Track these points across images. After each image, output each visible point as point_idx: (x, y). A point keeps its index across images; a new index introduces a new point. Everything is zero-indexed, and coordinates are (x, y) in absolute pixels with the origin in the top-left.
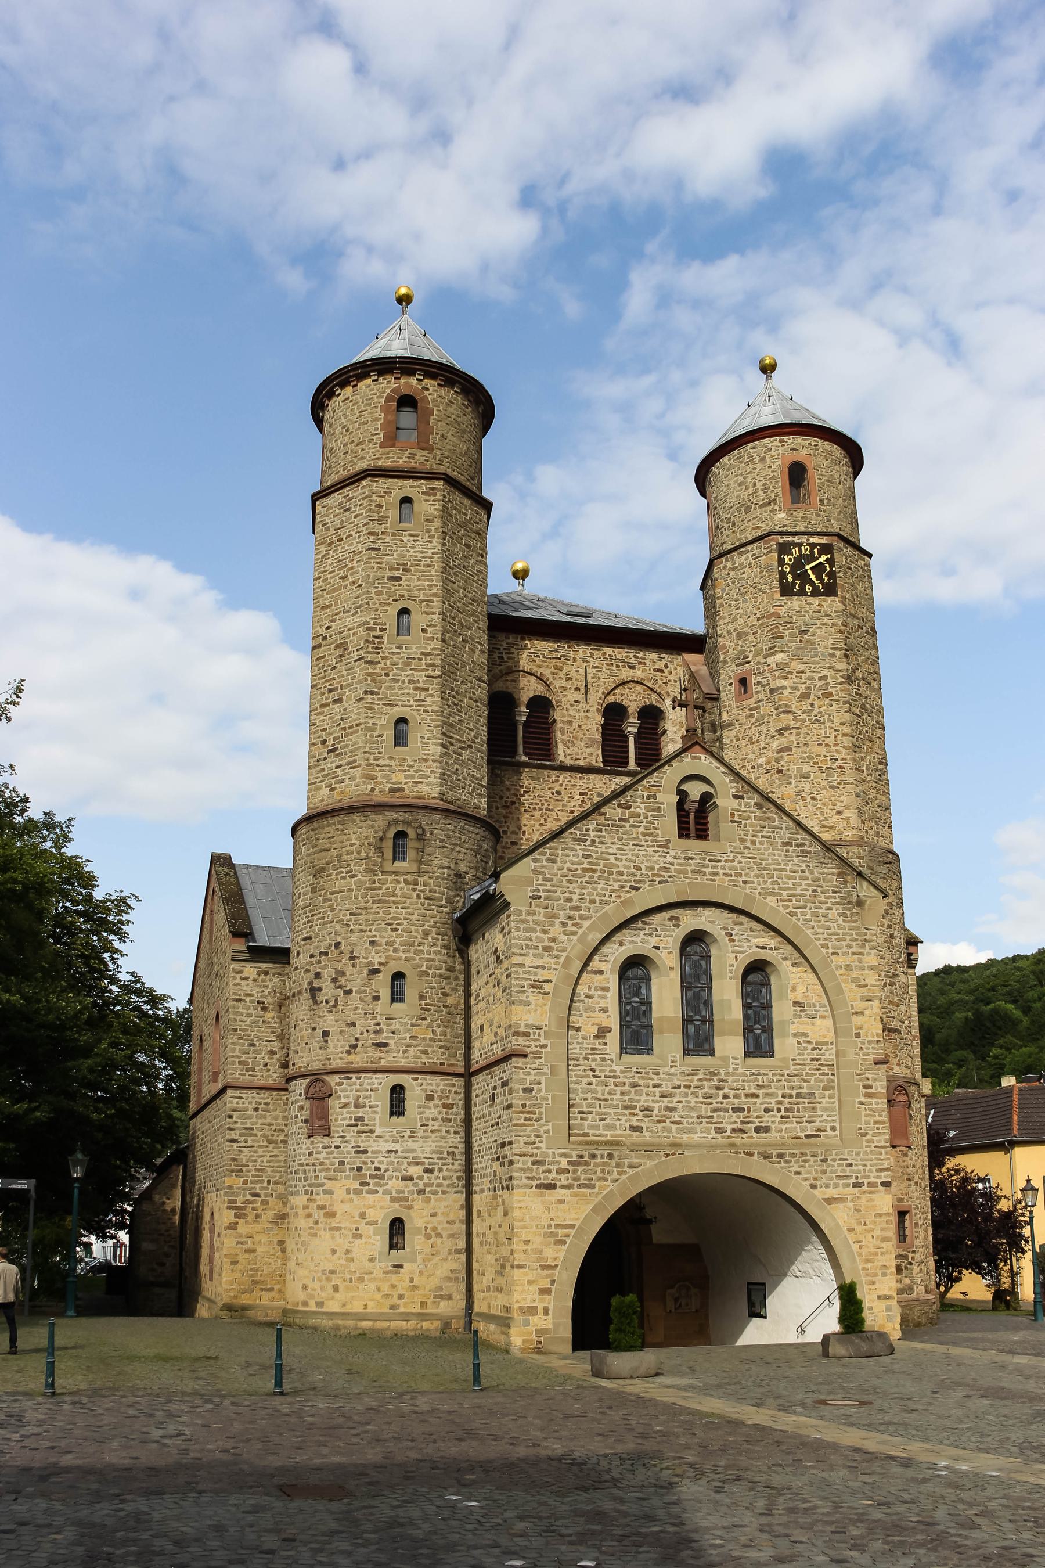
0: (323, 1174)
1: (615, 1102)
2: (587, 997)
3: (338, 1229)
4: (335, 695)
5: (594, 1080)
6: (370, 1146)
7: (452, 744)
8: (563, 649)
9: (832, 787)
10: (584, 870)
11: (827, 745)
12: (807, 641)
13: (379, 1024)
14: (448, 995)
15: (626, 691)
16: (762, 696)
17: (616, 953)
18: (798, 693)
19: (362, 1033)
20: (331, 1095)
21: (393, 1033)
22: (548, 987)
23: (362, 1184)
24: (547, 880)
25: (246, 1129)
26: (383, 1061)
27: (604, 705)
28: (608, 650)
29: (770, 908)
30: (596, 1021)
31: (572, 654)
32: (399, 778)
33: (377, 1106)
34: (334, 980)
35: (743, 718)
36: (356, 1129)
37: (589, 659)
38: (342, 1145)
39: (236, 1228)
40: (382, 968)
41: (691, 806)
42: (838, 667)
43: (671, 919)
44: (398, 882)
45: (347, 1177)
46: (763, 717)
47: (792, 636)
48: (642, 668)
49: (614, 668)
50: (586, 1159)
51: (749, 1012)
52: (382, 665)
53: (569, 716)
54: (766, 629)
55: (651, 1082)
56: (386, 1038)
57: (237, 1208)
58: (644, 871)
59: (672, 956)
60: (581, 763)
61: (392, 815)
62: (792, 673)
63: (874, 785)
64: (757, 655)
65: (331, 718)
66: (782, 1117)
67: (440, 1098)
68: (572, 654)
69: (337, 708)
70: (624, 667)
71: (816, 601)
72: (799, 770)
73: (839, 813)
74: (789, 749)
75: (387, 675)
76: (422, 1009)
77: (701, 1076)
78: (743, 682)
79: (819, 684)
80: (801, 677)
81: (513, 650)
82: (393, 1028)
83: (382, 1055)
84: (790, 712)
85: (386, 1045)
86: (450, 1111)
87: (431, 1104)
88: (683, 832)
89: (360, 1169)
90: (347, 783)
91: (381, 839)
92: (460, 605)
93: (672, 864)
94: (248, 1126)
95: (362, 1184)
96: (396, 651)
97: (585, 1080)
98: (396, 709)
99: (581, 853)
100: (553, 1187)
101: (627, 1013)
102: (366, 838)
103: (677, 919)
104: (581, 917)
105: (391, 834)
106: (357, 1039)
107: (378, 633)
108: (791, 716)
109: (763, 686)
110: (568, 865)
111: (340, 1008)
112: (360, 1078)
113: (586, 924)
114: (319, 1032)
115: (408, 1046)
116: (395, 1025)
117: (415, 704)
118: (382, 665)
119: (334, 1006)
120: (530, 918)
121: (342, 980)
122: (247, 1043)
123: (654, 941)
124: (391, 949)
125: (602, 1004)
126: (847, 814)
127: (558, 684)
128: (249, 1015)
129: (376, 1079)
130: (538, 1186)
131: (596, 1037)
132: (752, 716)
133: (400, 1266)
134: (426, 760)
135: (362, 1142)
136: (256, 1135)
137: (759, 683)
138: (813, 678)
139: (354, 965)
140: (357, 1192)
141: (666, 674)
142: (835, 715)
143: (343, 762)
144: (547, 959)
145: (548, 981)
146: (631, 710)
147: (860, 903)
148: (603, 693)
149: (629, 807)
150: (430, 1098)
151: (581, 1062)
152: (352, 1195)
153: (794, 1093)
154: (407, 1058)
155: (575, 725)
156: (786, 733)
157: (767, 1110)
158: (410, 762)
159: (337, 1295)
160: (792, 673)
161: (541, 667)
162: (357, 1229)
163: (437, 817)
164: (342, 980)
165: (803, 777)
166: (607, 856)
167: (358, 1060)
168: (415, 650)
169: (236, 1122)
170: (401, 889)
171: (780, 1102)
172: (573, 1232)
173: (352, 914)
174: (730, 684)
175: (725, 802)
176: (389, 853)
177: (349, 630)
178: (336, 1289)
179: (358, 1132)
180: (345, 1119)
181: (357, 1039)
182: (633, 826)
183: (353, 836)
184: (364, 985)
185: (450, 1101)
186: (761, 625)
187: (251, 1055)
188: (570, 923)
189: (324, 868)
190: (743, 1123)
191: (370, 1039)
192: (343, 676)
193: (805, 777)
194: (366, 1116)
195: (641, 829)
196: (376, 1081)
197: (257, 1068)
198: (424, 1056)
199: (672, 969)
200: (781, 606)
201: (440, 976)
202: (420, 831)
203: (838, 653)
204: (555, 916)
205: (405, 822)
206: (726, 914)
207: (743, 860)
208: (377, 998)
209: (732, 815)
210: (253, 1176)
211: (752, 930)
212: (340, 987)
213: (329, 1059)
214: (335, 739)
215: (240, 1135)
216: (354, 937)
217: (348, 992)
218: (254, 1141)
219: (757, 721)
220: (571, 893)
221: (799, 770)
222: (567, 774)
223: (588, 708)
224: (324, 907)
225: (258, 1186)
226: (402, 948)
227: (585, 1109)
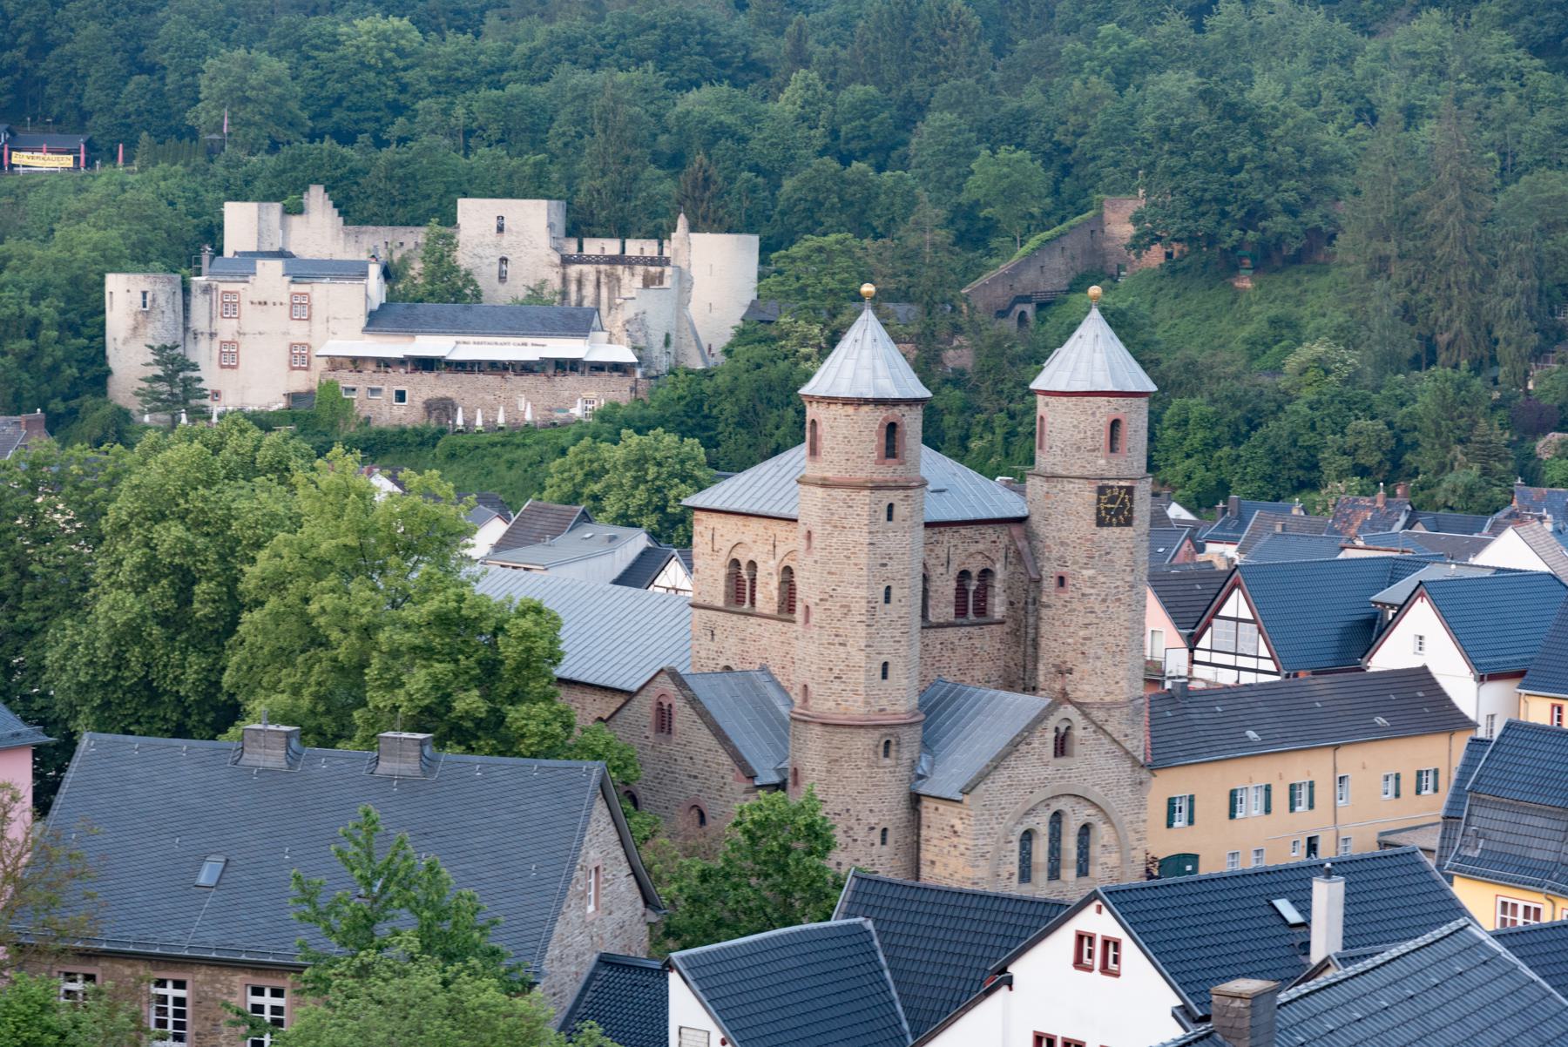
15: (971, 560)
16: (1075, 595)
17: (1021, 829)
22: (988, 856)
29: (1096, 794)
31: (941, 538)
32: (884, 703)
34: (845, 832)
35: (1059, 604)
46: (1074, 610)
47: (1100, 556)
60: (941, 620)
61: (885, 731)
64: (1074, 563)
68: (941, 538)
69: (841, 649)
71: (1117, 530)
74: (1090, 639)
78: (1061, 581)
105: (882, 743)
113: (1007, 817)
121: (851, 833)
123: (1037, 820)
126: (1122, 683)
147: (1141, 783)
163: (906, 728)
164: (851, 833)
168: (895, 616)
170: (887, 777)
175: (1078, 733)
176: (881, 754)
193: (1098, 658)
203: (1128, 569)
205: (891, 735)
206: (1073, 799)
208: (873, 845)
216: (859, 807)
217: (855, 840)
222: (932, 630)
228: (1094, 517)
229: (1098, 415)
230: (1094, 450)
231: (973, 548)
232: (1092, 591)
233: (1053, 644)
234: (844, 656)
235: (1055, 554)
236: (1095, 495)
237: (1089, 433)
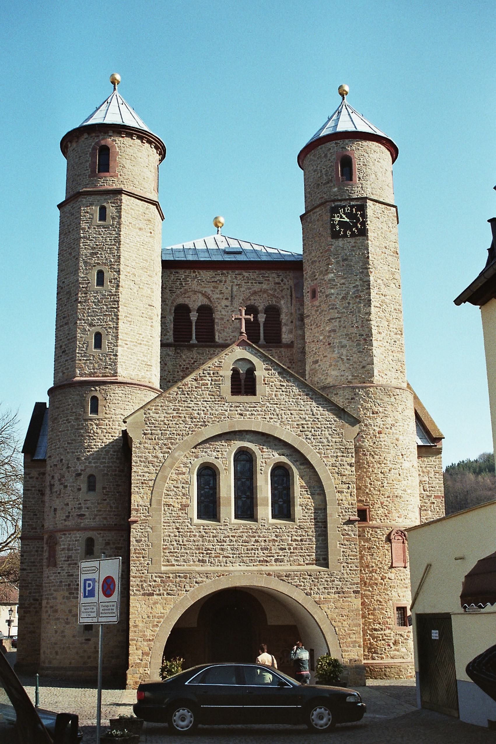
0: (53, 588)
1: (190, 546)
3: (58, 619)
4: (65, 321)
6: (75, 572)
7: (127, 344)
9: (359, 352)
12: (347, 265)
13: (80, 504)
14: (120, 486)
15: (257, 297)
18: (340, 297)
19: (72, 509)
20: (56, 544)
21: (88, 508)
23: (70, 593)
25: (31, 562)
26: (82, 524)
28: (246, 274)
30: (179, 501)
31: (224, 279)
33: (78, 550)
36: (68, 562)
37: (234, 280)
38: (61, 572)
39: (24, 619)
40: (82, 472)
41: (243, 377)
45: (63, 590)
46: (322, 311)
49: (250, 284)
50: (171, 579)
51: (276, 492)
53: (222, 315)
54: (325, 259)
56: (84, 511)
57: (26, 608)
63: (390, 348)
66: (291, 553)
67: (114, 543)
68: (224, 279)
70: (256, 283)
72: (340, 342)
73: (364, 367)
74: (334, 331)
76: (104, 494)
81: (188, 279)
82: (87, 505)
83: (82, 521)
84: (336, 308)
85: (84, 515)
86: (120, 551)
87: (108, 547)
88: (236, 390)
89: (69, 585)
92: (133, 264)
93: (226, 411)
94: (32, 560)
95: (70, 593)
97: (173, 535)
100: (152, 594)
102: (76, 401)
104: (172, 444)
106: (69, 513)
109: (322, 293)
111: (62, 495)
112: (70, 534)
114: (53, 508)
115: (96, 515)
116: (89, 504)
119: (59, 494)
122: (32, 514)
124: (88, 462)
128: (34, 498)
129: (78, 534)
130: (144, 595)
133: (89, 640)
135: (71, 569)
136: (36, 566)
139: (69, 472)
140: (68, 598)
141: (282, 284)
146: (260, 309)
148: (243, 300)
150: (107, 544)
152: (65, 600)
153: (299, 538)
154: (95, 522)
155: (225, 320)
156: (333, 321)
157: (282, 549)
159: (58, 657)
161: (205, 287)
162: (67, 619)
165: (342, 347)
166: (189, 409)
167: (70, 524)
169: (25, 559)
171: (291, 545)
172: (162, 620)
173: (68, 443)
177: (72, 284)
178: (57, 653)
179: (69, 564)
180: (63, 557)
181: (69, 513)
183: (70, 400)
184: (73, 482)
185: (120, 545)
186: (322, 256)
187: (35, 521)
189: (56, 418)
190: (267, 556)
191: (75, 512)
194: (73, 555)
196: (78, 535)
197: (38, 528)
198: (105, 521)
200: (332, 245)
201: (115, 475)
207: (270, 405)
208: (79, 489)
209: (264, 380)
210: (35, 589)
211: (275, 445)
212: (61, 484)
213: (56, 524)
214: (65, 345)
215: (28, 566)
217: (66, 487)
218: (35, 569)
219: (320, 313)
221: (340, 342)
224: (56, 439)
225: (37, 594)
226: (93, 461)
227: (172, 550)
228: (329, 231)
229: (329, 155)
230: (328, 183)
231: (257, 287)
232: (333, 291)
233: (313, 345)
236: (329, 214)
237: (323, 171)
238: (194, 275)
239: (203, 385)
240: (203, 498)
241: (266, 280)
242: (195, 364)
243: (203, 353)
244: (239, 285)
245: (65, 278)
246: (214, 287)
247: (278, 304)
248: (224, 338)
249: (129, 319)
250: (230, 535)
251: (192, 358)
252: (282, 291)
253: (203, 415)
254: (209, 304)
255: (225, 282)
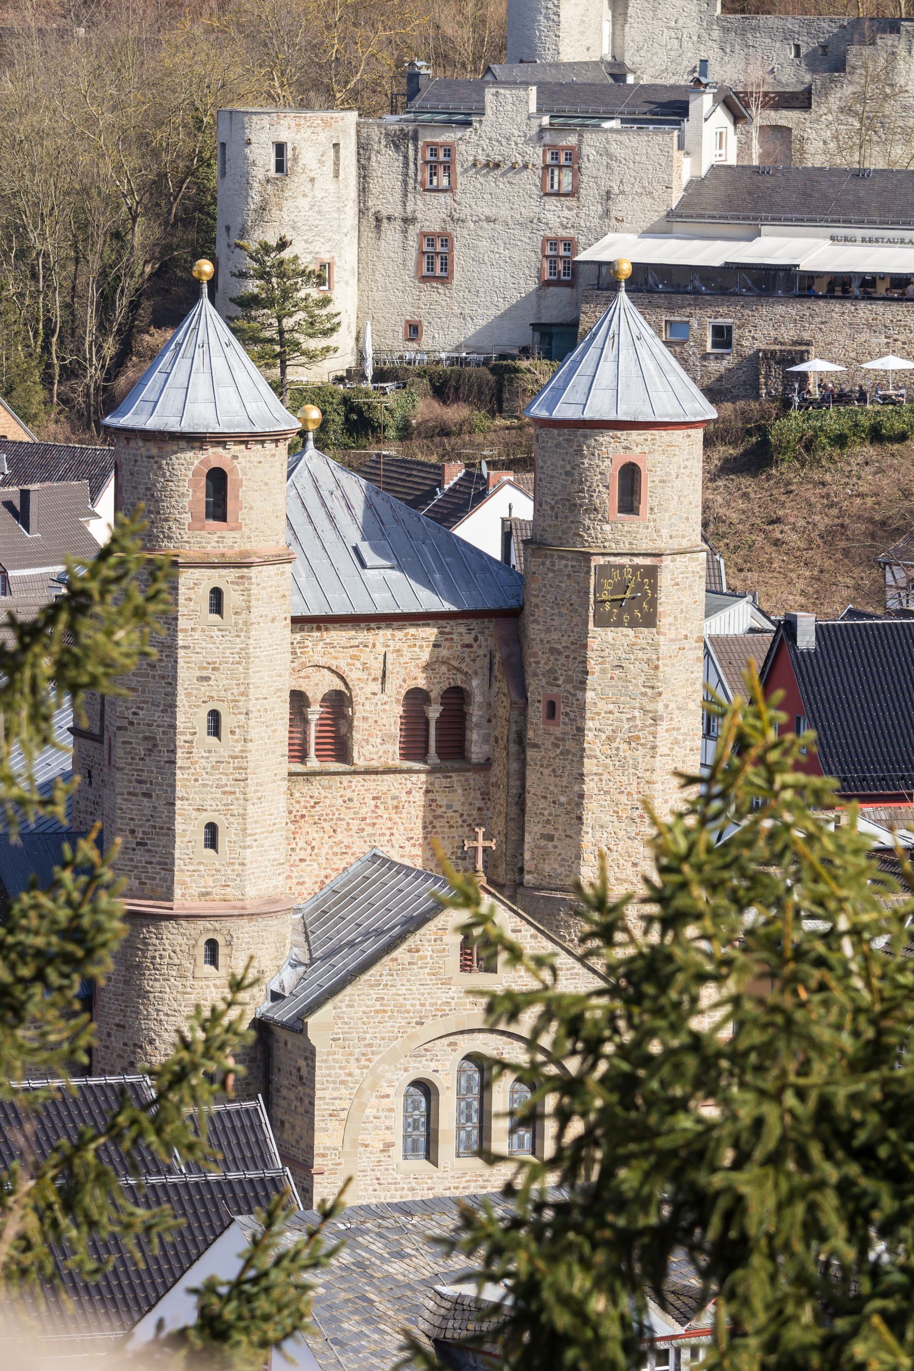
2: (375, 1118)
5: (378, 1187)
8: (362, 636)
10: (377, 1012)
11: (629, 794)
18: (604, 736)
22: (343, 1115)
24: (346, 1023)
27: (404, 692)
28: (412, 631)
30: (380, 1137)
35: (548, 744)
42: (648, 708)
43: (450, 1044)
44: (208, 986)
48: (447, 644)
49: (417, 649)
52: (192, 771)
55: (426, 1186)
58: (428, 1008)
59: (450, 1077)
60: (375, 764)
62: (598, 714)
65: (139, 810)
75: (196, 780)
77: (468, 1178)
79: (627, 726)
80: (608, 719)
81: (307, 643)
90: (157, 881)
91: (194, 946)
96: (206, 755)
97: (371, 1188)
98: (205, 814)
99: (374, 997)
101: (409, 1126)
103: (456, 1044)
104: (373, 1053)
107: (188, 738)
108: (594, 761)
109: (570, 720)
110: (364, 1008)
113: (376, 1058)
117: (223, 808)
118: (192, 771)
120: (331, 1058)
123: (433, 1065)
125: (388, 1123)
127: (354, 676)
131: (382, 1151)
132: (557, 746)
134: (232, 864)
137: (567, 714)
138: (621, 721)
142: (640, 760)
143: (154, 860)
144: (343, 1091)
145: (343, 1110)
149: (418, 951)
151: (369, 1173)
158: (217, 866)
160: (598, 714)
174: (539, 701)
182: (421, 968)
188: (363, 1058)
192: (152, 772)
195: (427, 970)
199: (448, 1088)
202: (228, 938)
204: (351, 1054)
214: (144, 833)
219: (562, 753)
220: (365, 1032)
222: (359, 778)
223: (386, 699)
234: (147, 812)
235: (543, 667)
238: (319, 634)
239: (421, 958)
240: (409, 1130)
241: (446, 639)
242: (317, 808)
243: (330, 787)
244: (398, 651)
245: (142, 709)
246: (354, 657)
247: (464, 686)
248: (368, 756)
249: (259, 794)
250: (452, 1185)
251: (311, 797)
252: (474, 661)
253: (418, 1007)
254: (343, 688)
255: (374, 646)
